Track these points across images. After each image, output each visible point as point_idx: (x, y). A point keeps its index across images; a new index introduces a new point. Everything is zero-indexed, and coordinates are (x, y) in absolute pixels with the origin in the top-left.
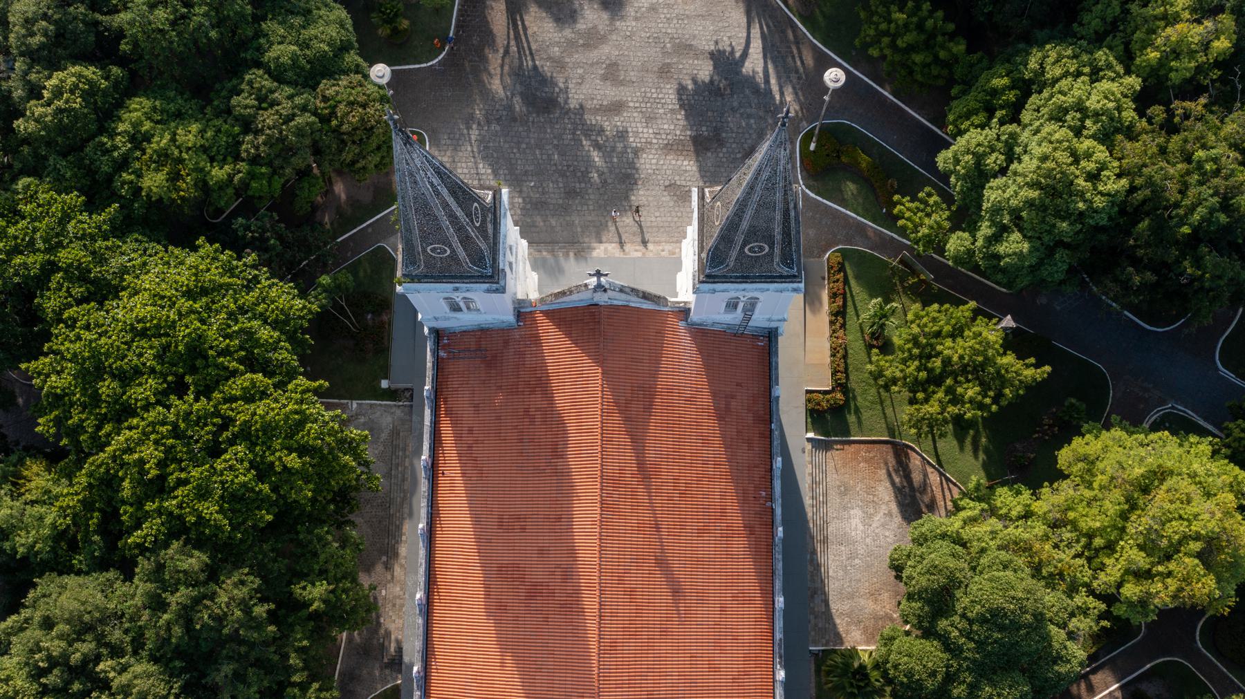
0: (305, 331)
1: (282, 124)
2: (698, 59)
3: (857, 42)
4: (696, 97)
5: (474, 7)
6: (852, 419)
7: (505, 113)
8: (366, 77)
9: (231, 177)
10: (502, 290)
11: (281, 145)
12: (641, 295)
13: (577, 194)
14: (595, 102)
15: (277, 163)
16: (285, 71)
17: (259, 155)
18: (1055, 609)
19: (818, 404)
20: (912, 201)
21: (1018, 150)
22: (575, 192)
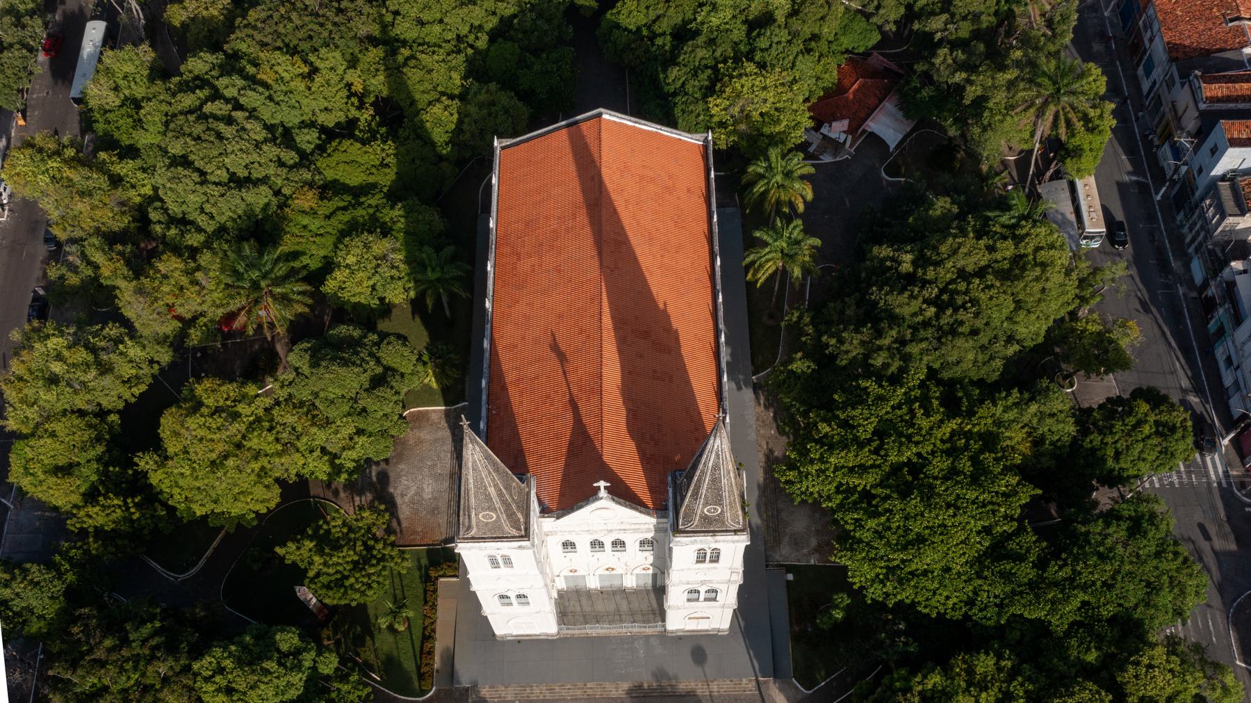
6: (424, 561)
18: (303, 383)
19: (449, 566)
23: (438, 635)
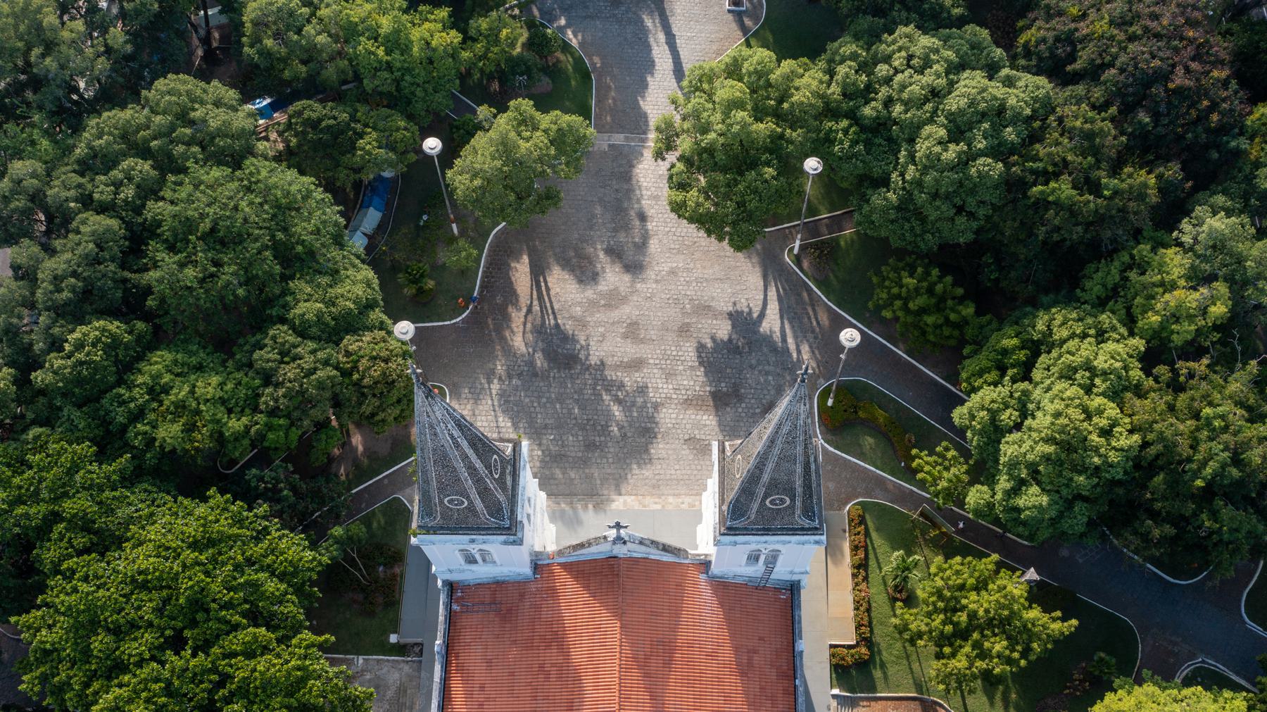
0: (313, 583)
1: (303, 378)
2: (716, 319)
3: (870, 305)
4: (715, 355)
5: (499, 269)
7: (526, 369)
8: (390, 333)
9: (247, 428)
10: (520, 542)
11: (301, 398)
12: (661, 547)
13: (597, 447)
14: (616, 358)
15: (296, 414)
16: (310, 327)
17: (278, 408)
20: (930, 455)
21: (1031, 406)
22: (595, 445)
23: (849, 572)
